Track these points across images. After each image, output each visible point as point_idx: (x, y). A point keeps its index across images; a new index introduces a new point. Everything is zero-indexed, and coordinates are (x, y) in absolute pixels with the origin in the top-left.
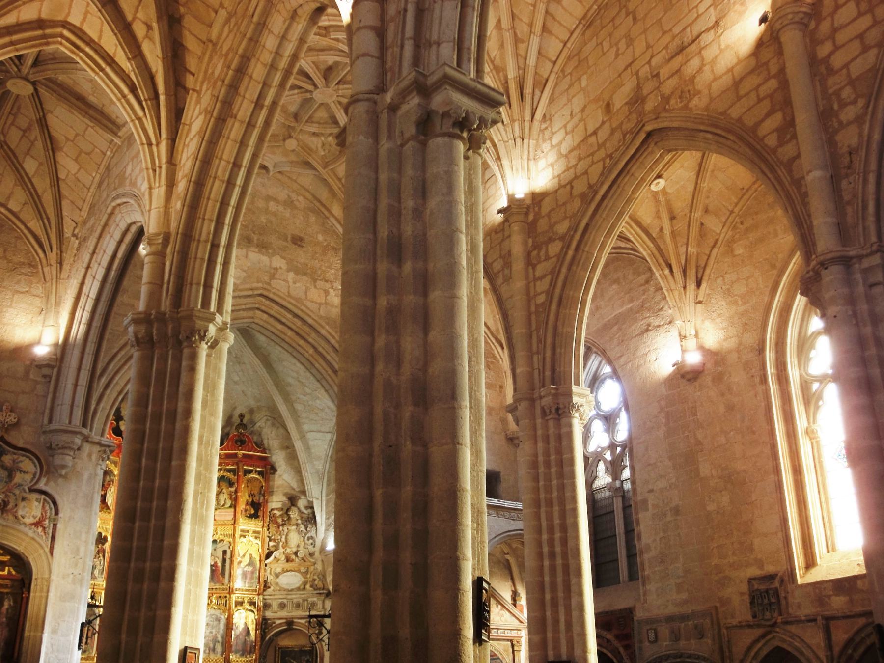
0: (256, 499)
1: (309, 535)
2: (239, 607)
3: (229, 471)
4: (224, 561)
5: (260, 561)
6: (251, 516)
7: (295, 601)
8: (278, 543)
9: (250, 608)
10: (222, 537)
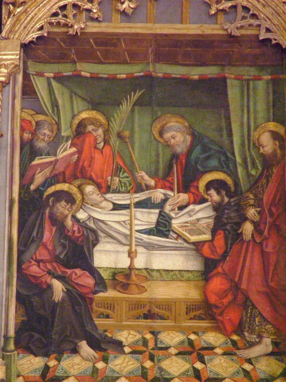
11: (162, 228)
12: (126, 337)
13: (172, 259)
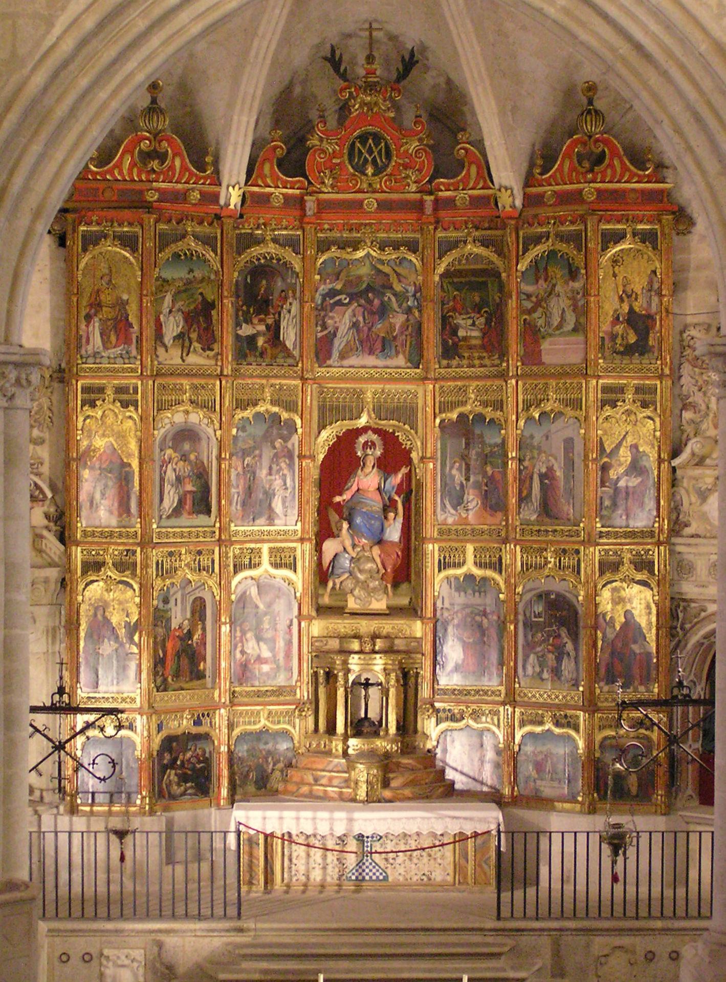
0: (639, 306)
2: (608, 576)
4: (570, 464)
5: (660, 461)
9: (639, 577)
11: (473, 324)
12: (466, 355)
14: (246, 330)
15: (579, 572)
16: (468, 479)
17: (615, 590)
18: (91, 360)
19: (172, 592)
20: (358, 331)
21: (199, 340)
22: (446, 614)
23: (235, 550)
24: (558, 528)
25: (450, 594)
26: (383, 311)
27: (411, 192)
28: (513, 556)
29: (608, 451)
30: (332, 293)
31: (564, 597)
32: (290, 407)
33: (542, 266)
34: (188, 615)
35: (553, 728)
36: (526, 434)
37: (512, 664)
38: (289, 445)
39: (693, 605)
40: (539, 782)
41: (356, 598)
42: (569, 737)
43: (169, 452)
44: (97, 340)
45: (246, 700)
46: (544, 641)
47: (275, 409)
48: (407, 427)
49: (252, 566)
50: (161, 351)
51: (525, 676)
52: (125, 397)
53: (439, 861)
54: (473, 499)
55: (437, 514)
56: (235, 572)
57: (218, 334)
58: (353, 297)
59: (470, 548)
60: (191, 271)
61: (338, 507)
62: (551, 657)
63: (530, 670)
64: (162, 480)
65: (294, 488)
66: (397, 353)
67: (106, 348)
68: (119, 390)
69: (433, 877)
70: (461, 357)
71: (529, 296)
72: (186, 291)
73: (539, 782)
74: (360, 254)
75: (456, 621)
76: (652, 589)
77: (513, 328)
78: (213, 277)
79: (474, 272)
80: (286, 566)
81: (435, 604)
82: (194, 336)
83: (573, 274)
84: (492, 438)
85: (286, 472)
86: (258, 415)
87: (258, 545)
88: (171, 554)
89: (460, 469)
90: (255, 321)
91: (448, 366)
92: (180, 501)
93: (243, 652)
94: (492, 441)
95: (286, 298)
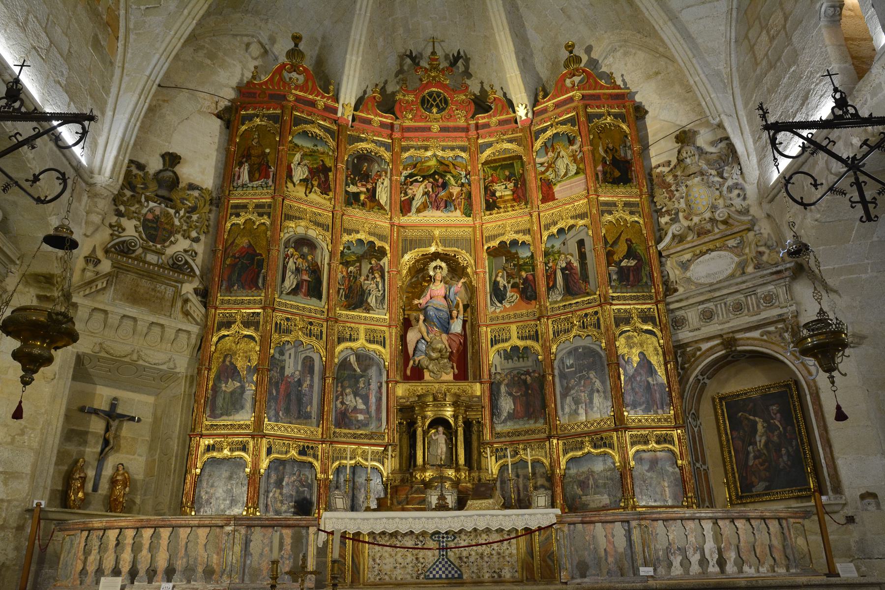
1: (730, 182)
3: (563, 123)
4: (582, 256)
6: (616, 182)
7: (730, 300)
8: (677, 214)
10: (572, 222)
11: (506, 188)
13: (509, 193)
14: (352, 189)
15: (599, 328)
16: (508, 282)
17: (629, 338)
18: (240, 189)
19: (287, 347)
20: (429, 196)
21: (319, 186)
22: (498, 377)
23: (338, 327)
24: (579, 300)
25: (501, 362)
26: (445, 185)
27: (462, 123)
28: (548, 327)
29: (611, 243)
30: (411, 175)
31: (589, 348)
32: (381, 238)
33: (549, 145)
34: (299, 368)
35: (592, 450)
36: (549, 245)
37: (553, 406)
38: (381, 263)
39: (688, 349)
40: (584, 498)
41: (430, 371)
42: (605, 454)
43: (291, 250)
44: (245, 177)
45: (344, 440)
46: (576, 385)
47: (372, 239)
48: (464, 251)
49: (351, 339)
50: (290, 185)
51: (563, 414)
52: (261, 210)
53: (508, 559)
54: (512, 295)
55: (489, 309)
56: (339, 343)
57: (332, 186)
58: (424, 178)
59: (513, 328)
60: (315, 145)
61: (418, 308)
62: (584, 396)
63: (567, 410)
64: (285, 267)
65: (384, 291)
66: (456, 209)
67: (251, 180)
68: (258, 206)
69: (503, 574)
70: (499, 208)
71: (542, 164)
72: (311, 155)
73: (584, 498)
74: (429, 154)
75: (506, 381)
76: (656, 336)
77: (533, 184)
78: (331, 153)
79: (504, 159)
80: (377, 343)
81: (490, 371)
82: (315, 183)
83: (571, 142)
84: (524, 254)
85: (378, 280)
86: (360, 241)
87: (357, 325)
88: (288, 319)
89: (502, 277)
90: (359, 185)
91: (491, 214)
92: (297, 285)
93: (342, 403)
94: (525, 256)
95: (380, 176)
